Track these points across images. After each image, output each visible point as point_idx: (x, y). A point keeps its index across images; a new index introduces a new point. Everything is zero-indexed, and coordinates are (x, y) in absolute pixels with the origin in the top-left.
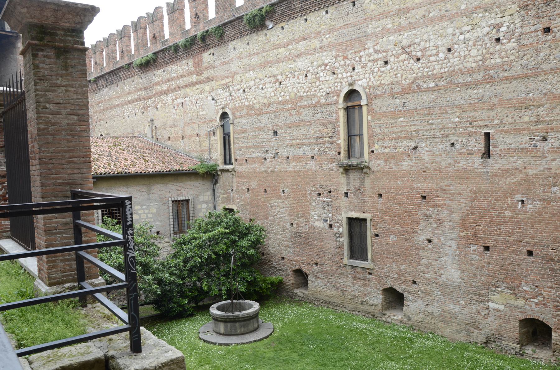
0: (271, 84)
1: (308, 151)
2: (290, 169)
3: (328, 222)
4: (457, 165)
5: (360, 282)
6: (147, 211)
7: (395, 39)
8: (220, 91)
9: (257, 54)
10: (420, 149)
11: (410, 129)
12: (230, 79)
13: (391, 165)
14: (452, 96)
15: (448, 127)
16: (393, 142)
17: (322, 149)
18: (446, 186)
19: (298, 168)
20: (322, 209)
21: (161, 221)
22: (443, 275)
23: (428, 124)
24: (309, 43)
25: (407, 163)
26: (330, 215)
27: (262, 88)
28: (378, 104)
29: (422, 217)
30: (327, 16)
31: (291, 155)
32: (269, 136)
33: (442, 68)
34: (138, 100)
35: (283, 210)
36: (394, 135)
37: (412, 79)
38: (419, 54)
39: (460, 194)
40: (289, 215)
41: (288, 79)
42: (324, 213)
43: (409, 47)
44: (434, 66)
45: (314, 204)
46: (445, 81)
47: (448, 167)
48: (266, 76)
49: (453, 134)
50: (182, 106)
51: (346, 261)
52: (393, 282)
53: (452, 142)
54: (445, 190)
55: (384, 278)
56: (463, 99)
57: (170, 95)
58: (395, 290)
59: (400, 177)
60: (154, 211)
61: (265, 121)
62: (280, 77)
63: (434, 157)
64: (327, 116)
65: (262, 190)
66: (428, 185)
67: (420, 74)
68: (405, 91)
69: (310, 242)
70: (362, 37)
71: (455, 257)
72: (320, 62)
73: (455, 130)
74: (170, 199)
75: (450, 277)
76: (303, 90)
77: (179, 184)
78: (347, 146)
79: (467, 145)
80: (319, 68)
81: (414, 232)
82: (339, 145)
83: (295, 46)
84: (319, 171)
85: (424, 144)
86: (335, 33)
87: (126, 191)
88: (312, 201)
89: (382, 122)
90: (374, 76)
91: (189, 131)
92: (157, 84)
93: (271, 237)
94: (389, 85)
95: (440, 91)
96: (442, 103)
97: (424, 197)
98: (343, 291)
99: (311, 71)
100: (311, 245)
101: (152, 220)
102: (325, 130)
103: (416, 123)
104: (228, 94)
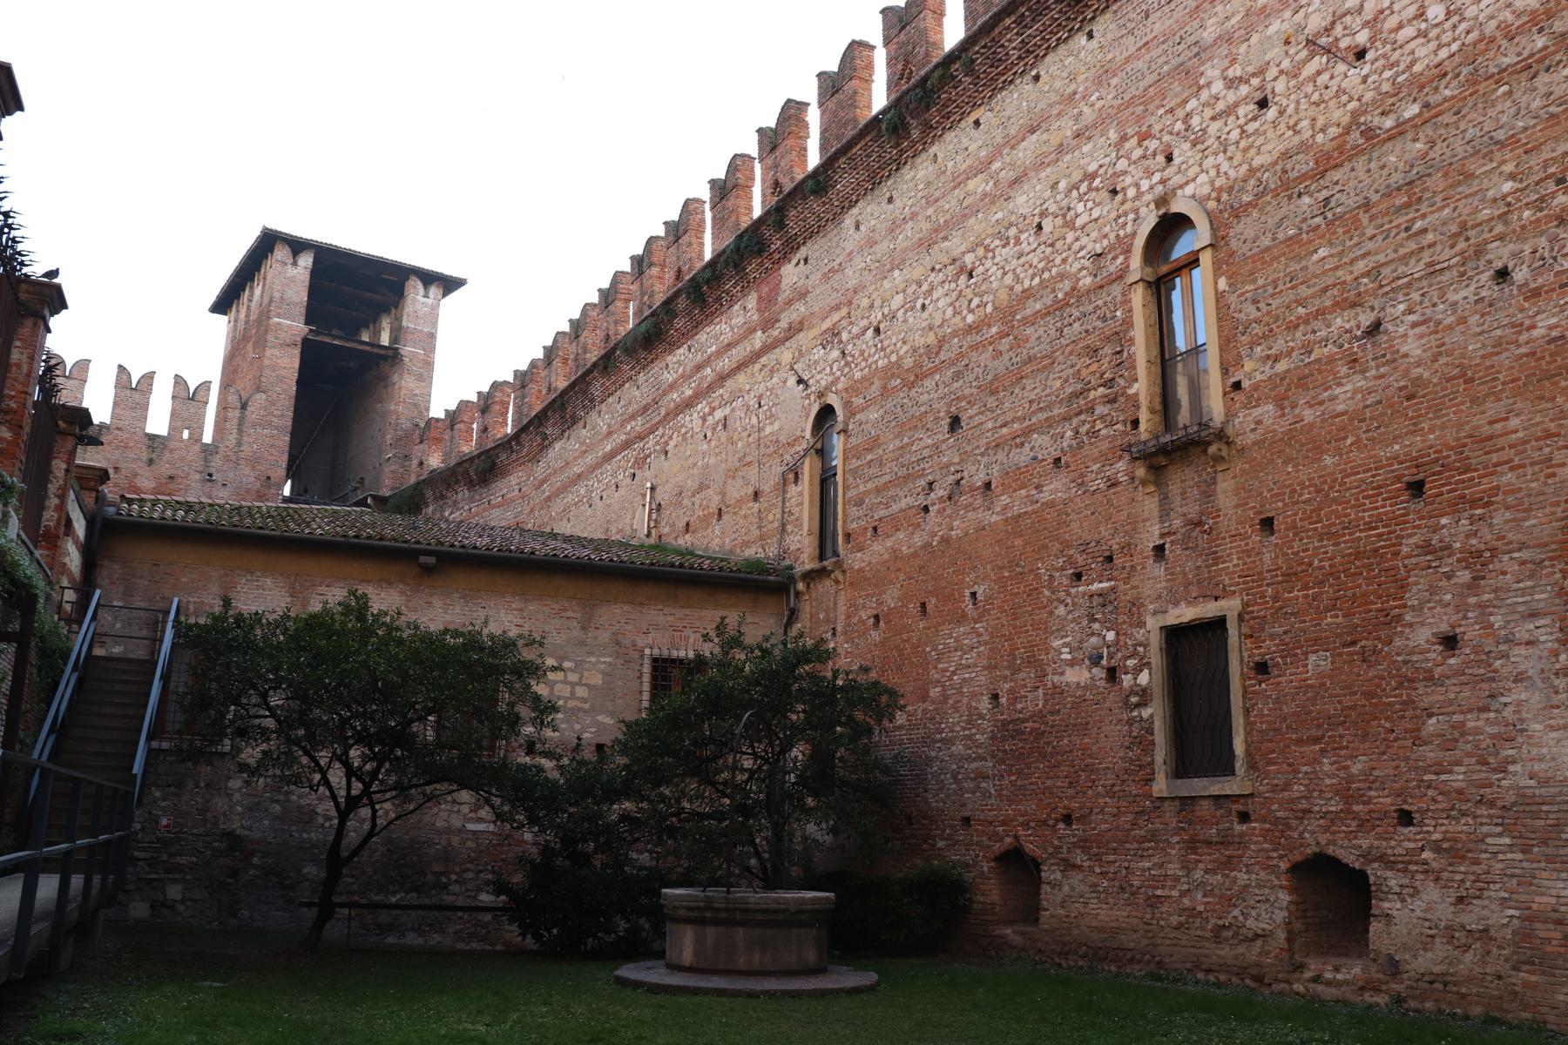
0: (947, 286)
1: (1045, 446)
2: (995, 518)
3: (1104, 662)
4: (1523, 337)
5: (1209, 858)
6: (573, 677)
7: (1286, 25)
8: (819, 353)
9: (911, 219)
10: (1390, 327)
11: (1351, 273)
12: (844, 311)
13: (1297, 411)
14: (1481, 119)
15: (1478, 221)
16: (1298, 334)
17: (1083, 430)
18: (1491, 423)
19: (1016, 510)
20: (1085, 623)
21: (611, 714)
22: (1514, 762)
23: (1408, 238)
24: (1045, 136)
25: (1349, 387)
26: (1111, 636)
27: (923, 307)
28: (1246, 232)
29: (1414, 560)
30: (1094, 43)
31: (996, 474)
32: (936, 437)
33: (1440, 47)
34: (626, 445)
35: (970, 658)
36: (1301, 310)
37: (1346, 120)
38: (1362, 38)
39: (1550, 435)
40: (985, 668)
41: (991, 254)
42: (1093, 634)
43: (1328, 30)
44: (1413, 52)
45: (1061, 610)
46: (1455, 83)
47: (1493, 354)
48: (933, 269)
49: (1501, 238)
50: (725, 426)
51: (1161, 786)
52: (1326, 830)
53: (1499, 265)
54: (1490, 438)
55: (1294, 823)
56: (1523, 113)
57: (700, 406)
58: (1334, 861)
59: (1329, 443)
60: (597, 680)
61: (928, 392)
62: (969, 259)
63: (1439, 336)
64: (1099, 324)
65: (913, 607)
66: (1432, 437)
67: (1369, 96)
68: (1326, 163)
69: (1048, 744)
70: (1190, 59)
71: (1557, 682)
72: (1077, 176)
73: (1506, 223)
74: (647, 651)
75: (1544, 766)
76: (1031, 271)
77: (680, 613)
78: (1158, 400)
79: (1555, 258)
80: (1075, 193)
81: (1390, 621)
82: (1134, 401)
83: (1007, 159)
84: (1077, 500)
85: (1402, 307)
86: (1114, 81)
87: (521, 610)
88: (1055, 604)
89: (1260, 282)
90: (1229, 154)
91: (737, 490)
92: (672, 387)
93: (933, 754)
94: (1275, 163)
95: (1440, 118)
96: (1449, 153)
97: (1417, 488)
98: (1154, 902)
99: (1053, 208)
100: (1052, 755)
101: (587, 706)
102: (1094, 367)
103: (1370, 245)
104: (836, 354)
